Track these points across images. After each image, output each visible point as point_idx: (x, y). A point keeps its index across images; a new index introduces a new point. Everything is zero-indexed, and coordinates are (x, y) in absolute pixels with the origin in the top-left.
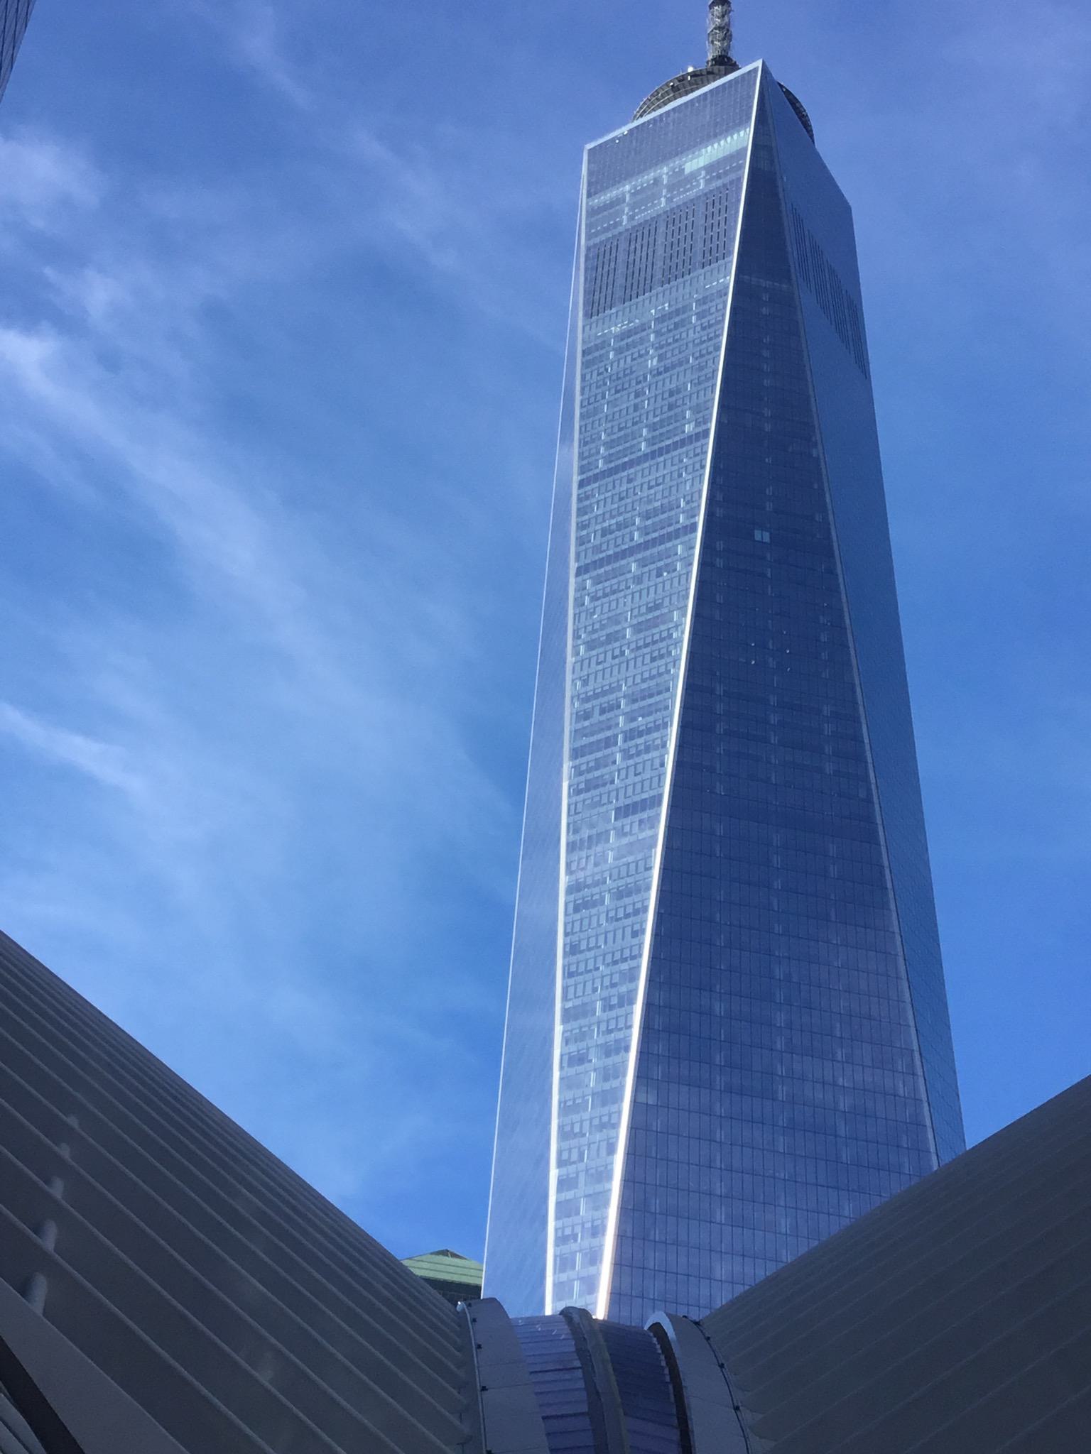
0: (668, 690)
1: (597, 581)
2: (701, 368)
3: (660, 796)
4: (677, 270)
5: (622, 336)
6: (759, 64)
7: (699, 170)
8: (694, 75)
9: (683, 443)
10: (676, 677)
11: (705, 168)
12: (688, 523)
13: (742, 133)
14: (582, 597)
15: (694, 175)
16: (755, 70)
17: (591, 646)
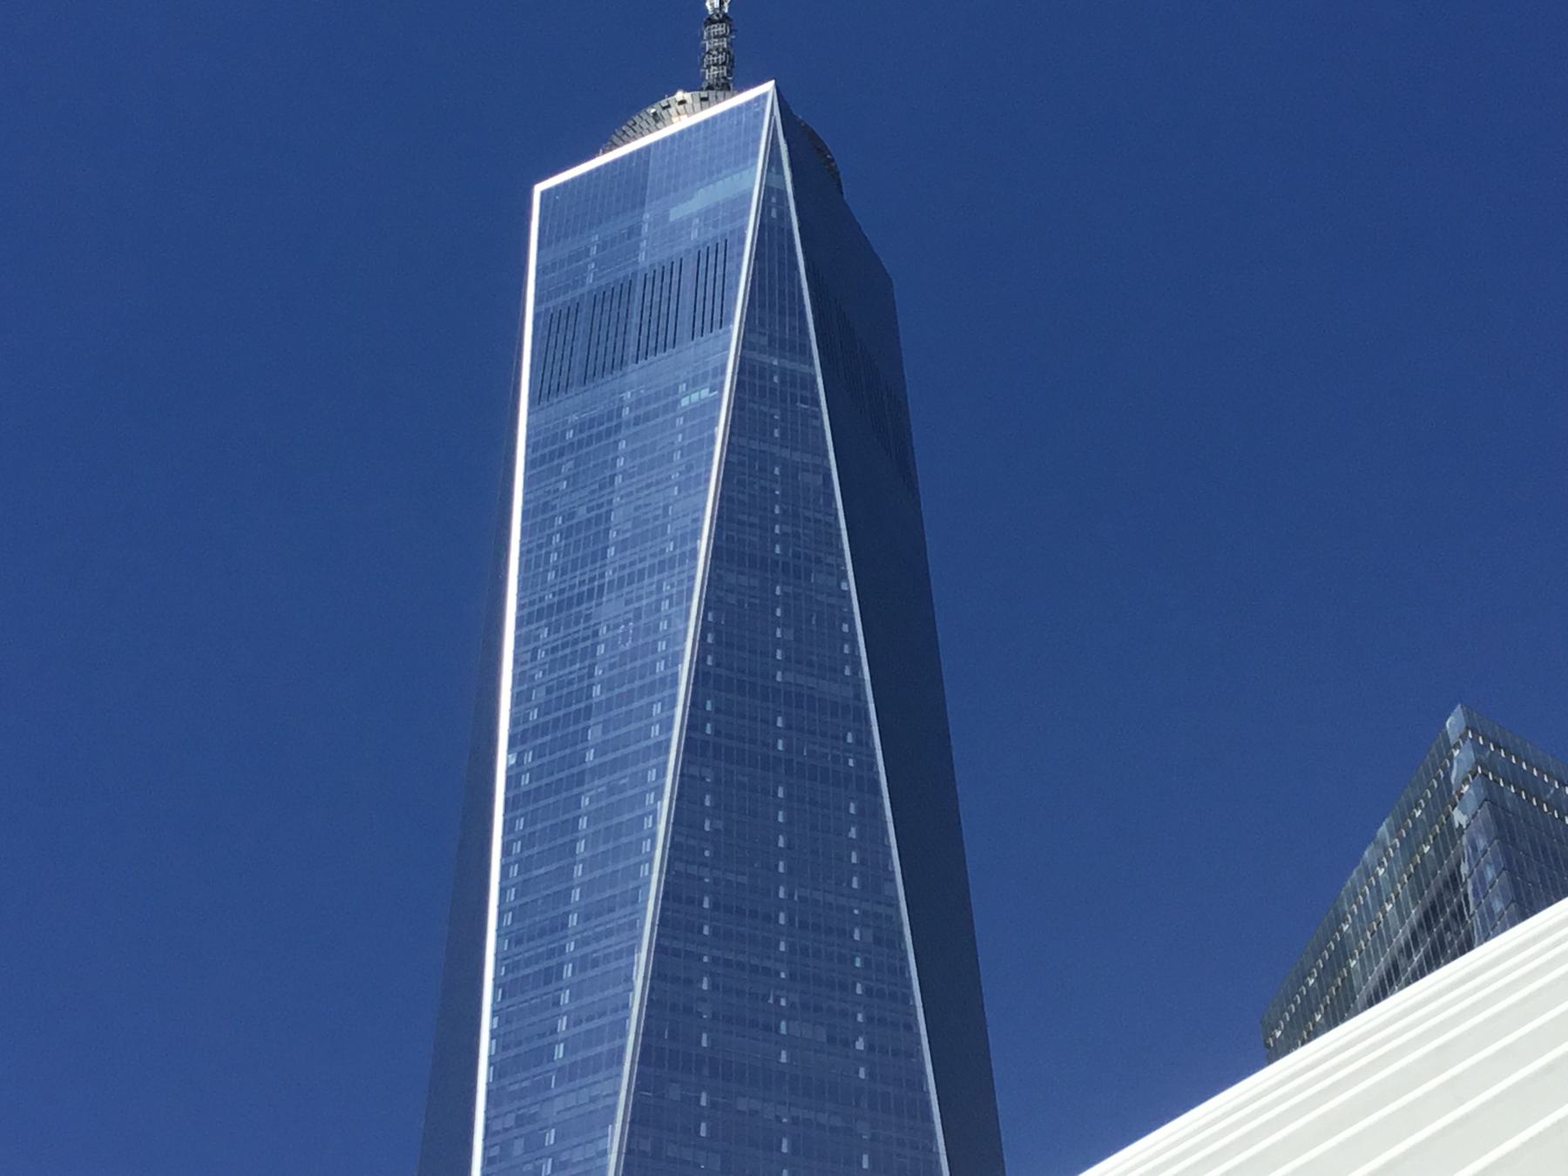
0: (635, 901)
1: (539, 754)
2: (690, 468)
3: (622, 1049)
4: (659, 341)
5: (579, 428)
6: (768, 87)
7: (690, 220)
8: (682, 102)
9: (661, 566)
10: (648, 882)
11: (699, 215)
12: (669, 672)
13: (746, 173)
14: (518, 777)
15: (686, 223)
16: (764, 96)
17: (528, 840)
